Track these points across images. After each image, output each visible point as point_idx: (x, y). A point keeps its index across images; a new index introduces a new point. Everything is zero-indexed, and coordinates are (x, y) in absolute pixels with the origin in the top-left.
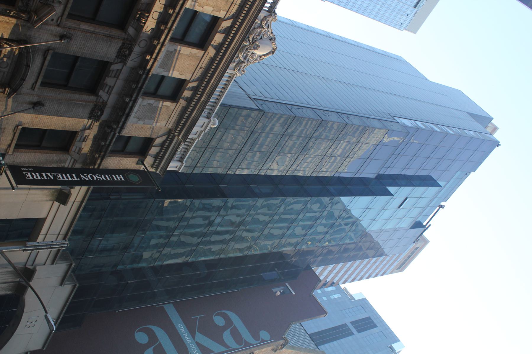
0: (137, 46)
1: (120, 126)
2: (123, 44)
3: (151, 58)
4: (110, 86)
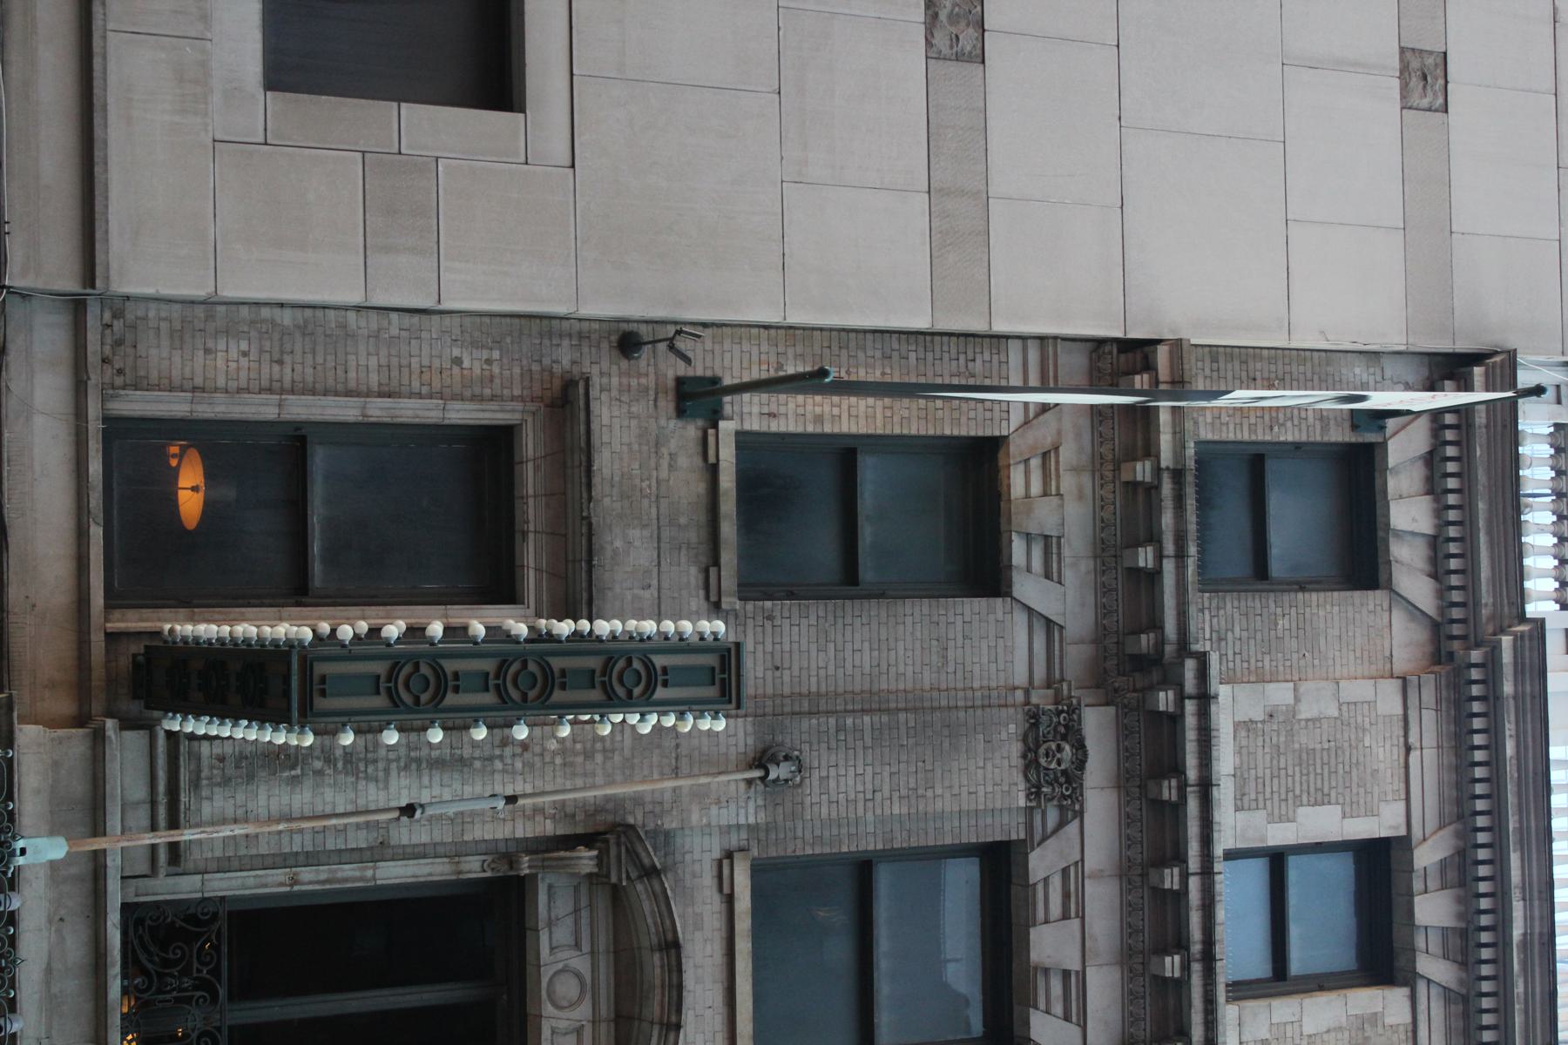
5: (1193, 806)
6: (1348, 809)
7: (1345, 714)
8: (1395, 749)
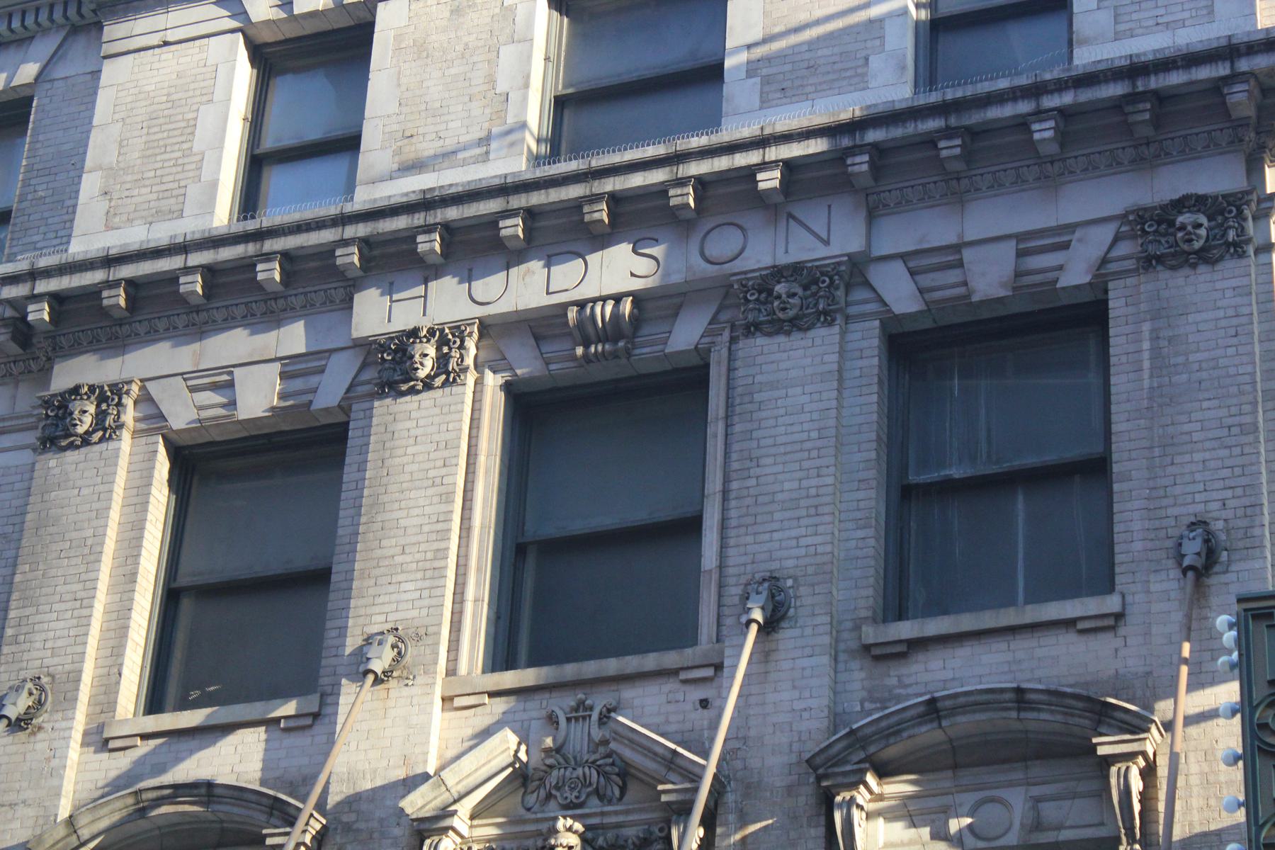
0: (738, 266)
1: (1222, 70)
2: (752, 329)
3: (764, 166)
4: (1021, 254)
5: (127, 271)
6: (205, 98)
7: (122, 115)
8: (164, 57)
